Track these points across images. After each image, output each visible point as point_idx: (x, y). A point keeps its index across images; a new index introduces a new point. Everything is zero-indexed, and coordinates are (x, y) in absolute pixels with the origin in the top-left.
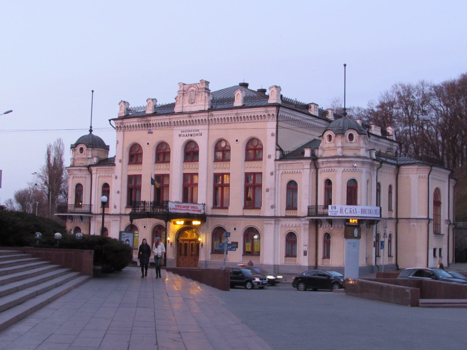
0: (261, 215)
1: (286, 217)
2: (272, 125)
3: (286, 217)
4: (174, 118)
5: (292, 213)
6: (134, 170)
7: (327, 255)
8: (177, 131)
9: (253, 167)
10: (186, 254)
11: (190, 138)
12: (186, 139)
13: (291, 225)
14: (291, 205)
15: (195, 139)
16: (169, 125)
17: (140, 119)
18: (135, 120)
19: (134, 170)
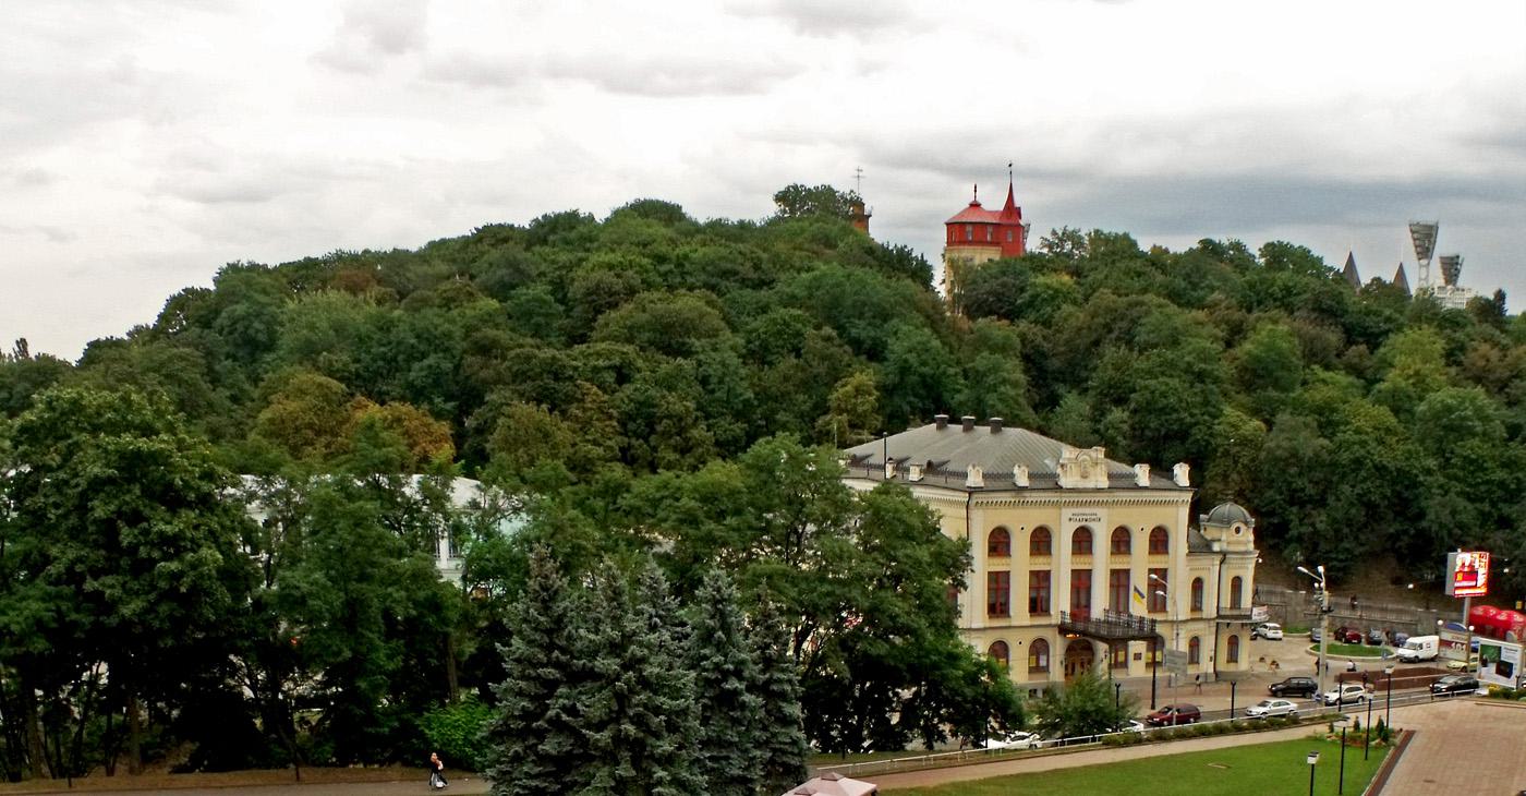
0: (1170, 618)
1: (1192, 620)
2: (1184, 512)
3: (1192, 620)
4: (1066, 497)
5: (1197, 615)
6: (999, 565)
7: (1233, 657)
8: (1067, 512)
9: (1159, 562)
10: (1073, 673)
11: (1084, 523)
12: (1078, 525)
13: (1198, 629)
14: (1197, 606)
15: (1091, 525)
16: (1057, 504)
17: (1013, 494)
18: (1004, 494)
19: (999, 565)
